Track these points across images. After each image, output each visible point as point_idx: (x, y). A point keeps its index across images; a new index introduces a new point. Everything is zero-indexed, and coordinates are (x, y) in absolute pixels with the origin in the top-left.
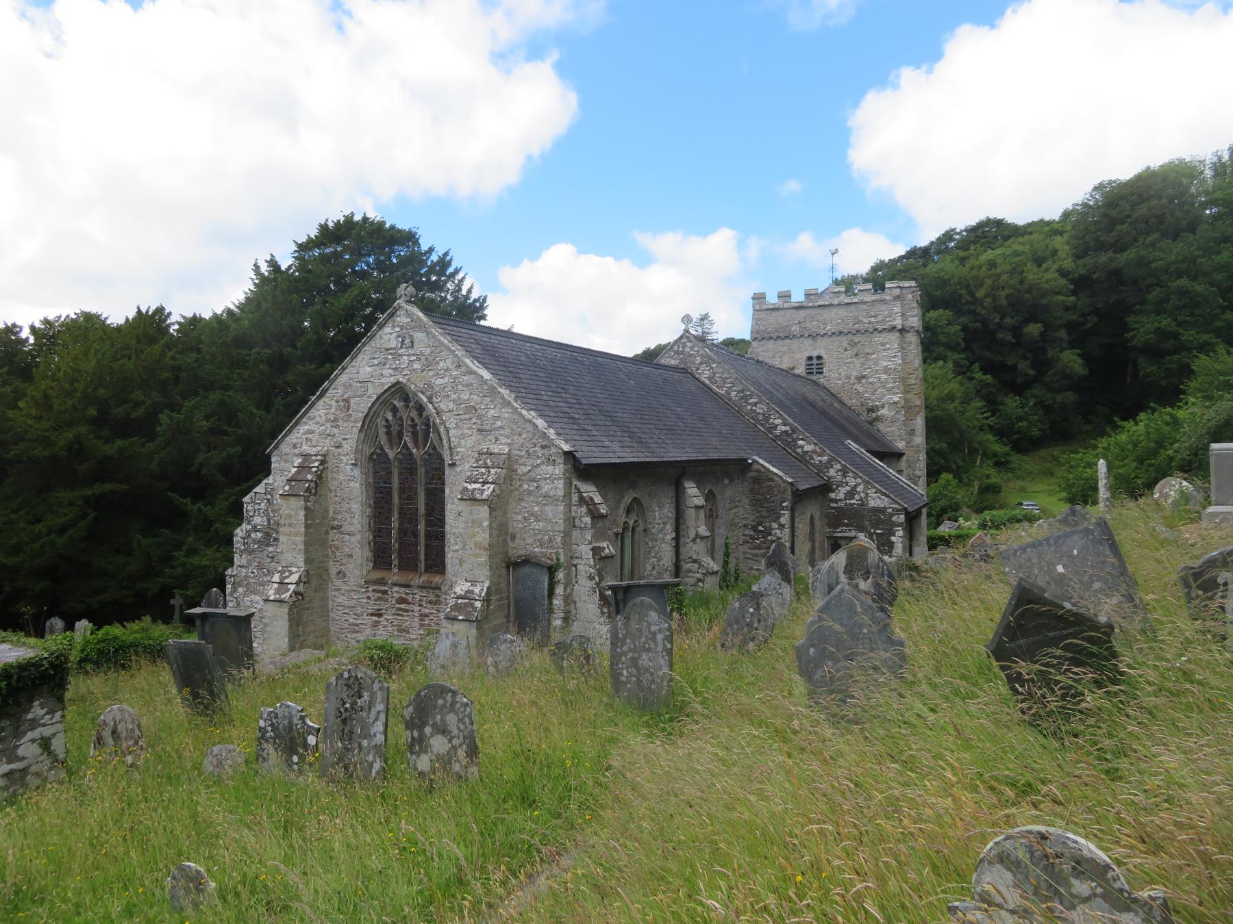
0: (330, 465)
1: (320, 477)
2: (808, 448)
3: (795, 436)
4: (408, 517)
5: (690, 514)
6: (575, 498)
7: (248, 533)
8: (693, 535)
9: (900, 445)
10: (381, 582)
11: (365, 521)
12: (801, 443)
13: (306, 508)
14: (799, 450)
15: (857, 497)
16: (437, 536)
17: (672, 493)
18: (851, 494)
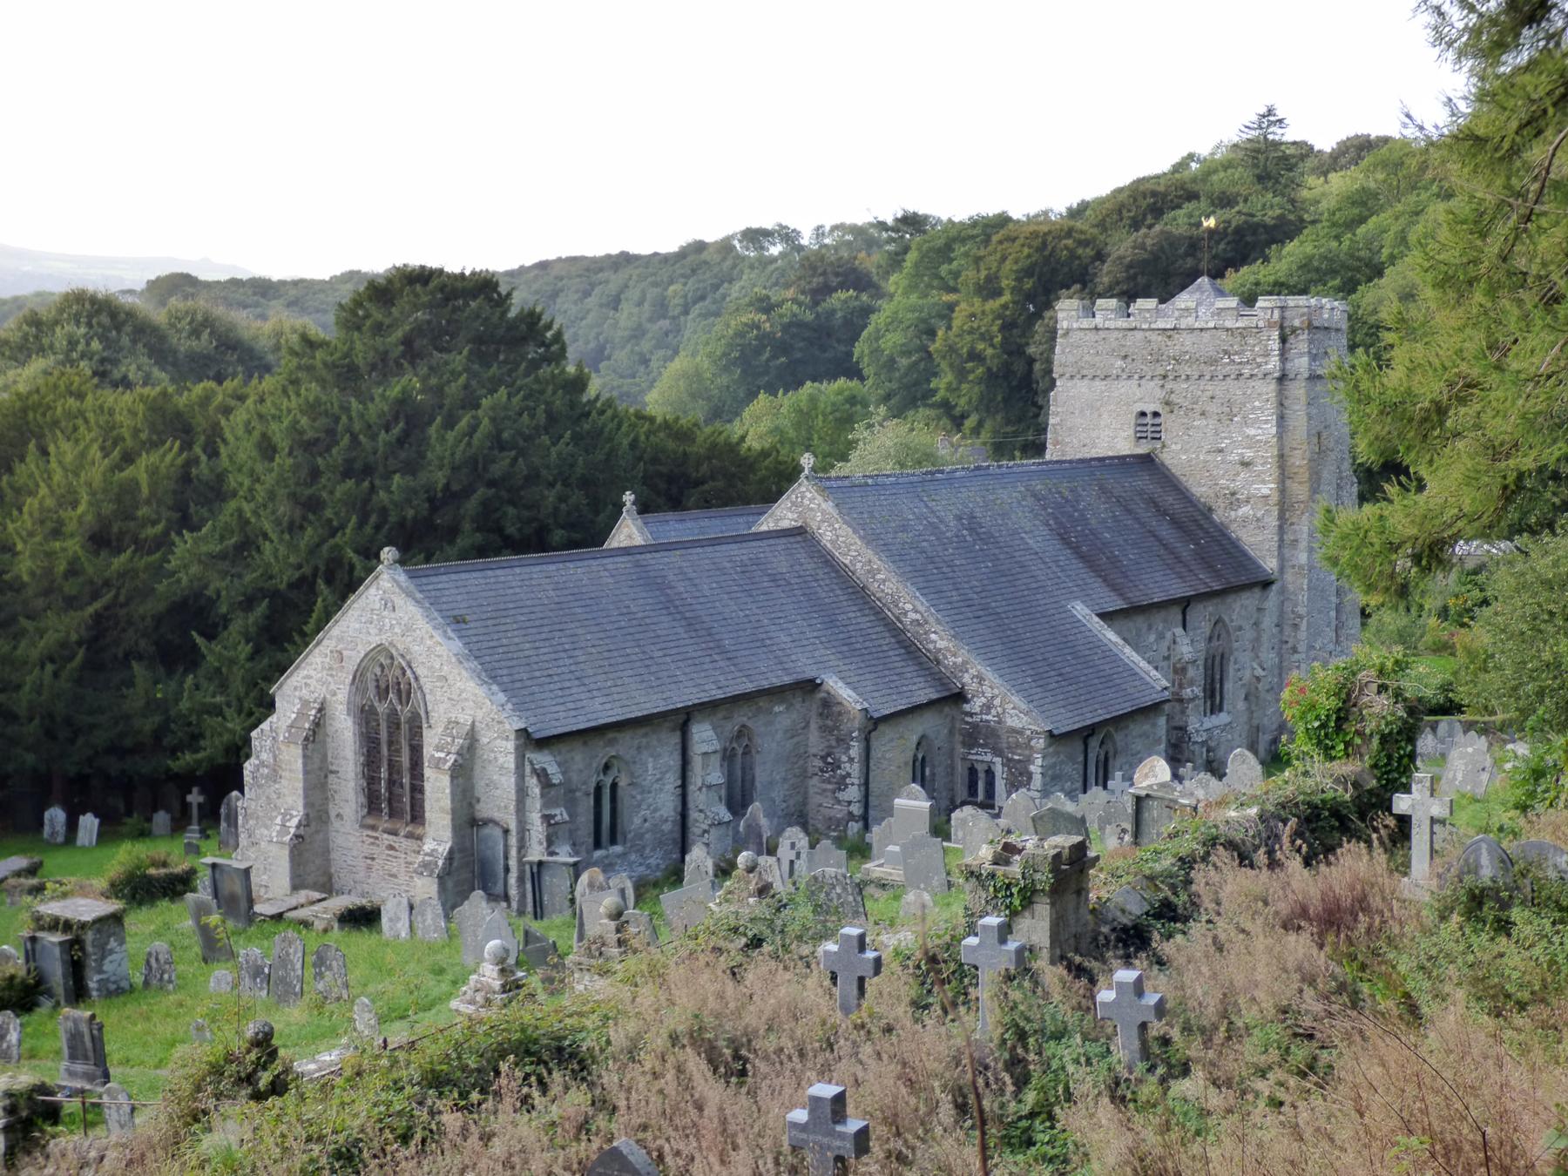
0: (328, 712)
1: (318, 725)
2: (941, 644)
3: (927, 627)
4: (393, 767)
5: (697, 763)
6: (528, 769)
7: (257, 767)
8: (699, 784)
9: (1270, 564)
10: (373, 828)
11: (359, 769)
12: (933, 636)
13: (305, 756)
14: (931, 646)
15: (993, 712)
16: (417, 789)
17: (676, 738)
18: (988, 707)
